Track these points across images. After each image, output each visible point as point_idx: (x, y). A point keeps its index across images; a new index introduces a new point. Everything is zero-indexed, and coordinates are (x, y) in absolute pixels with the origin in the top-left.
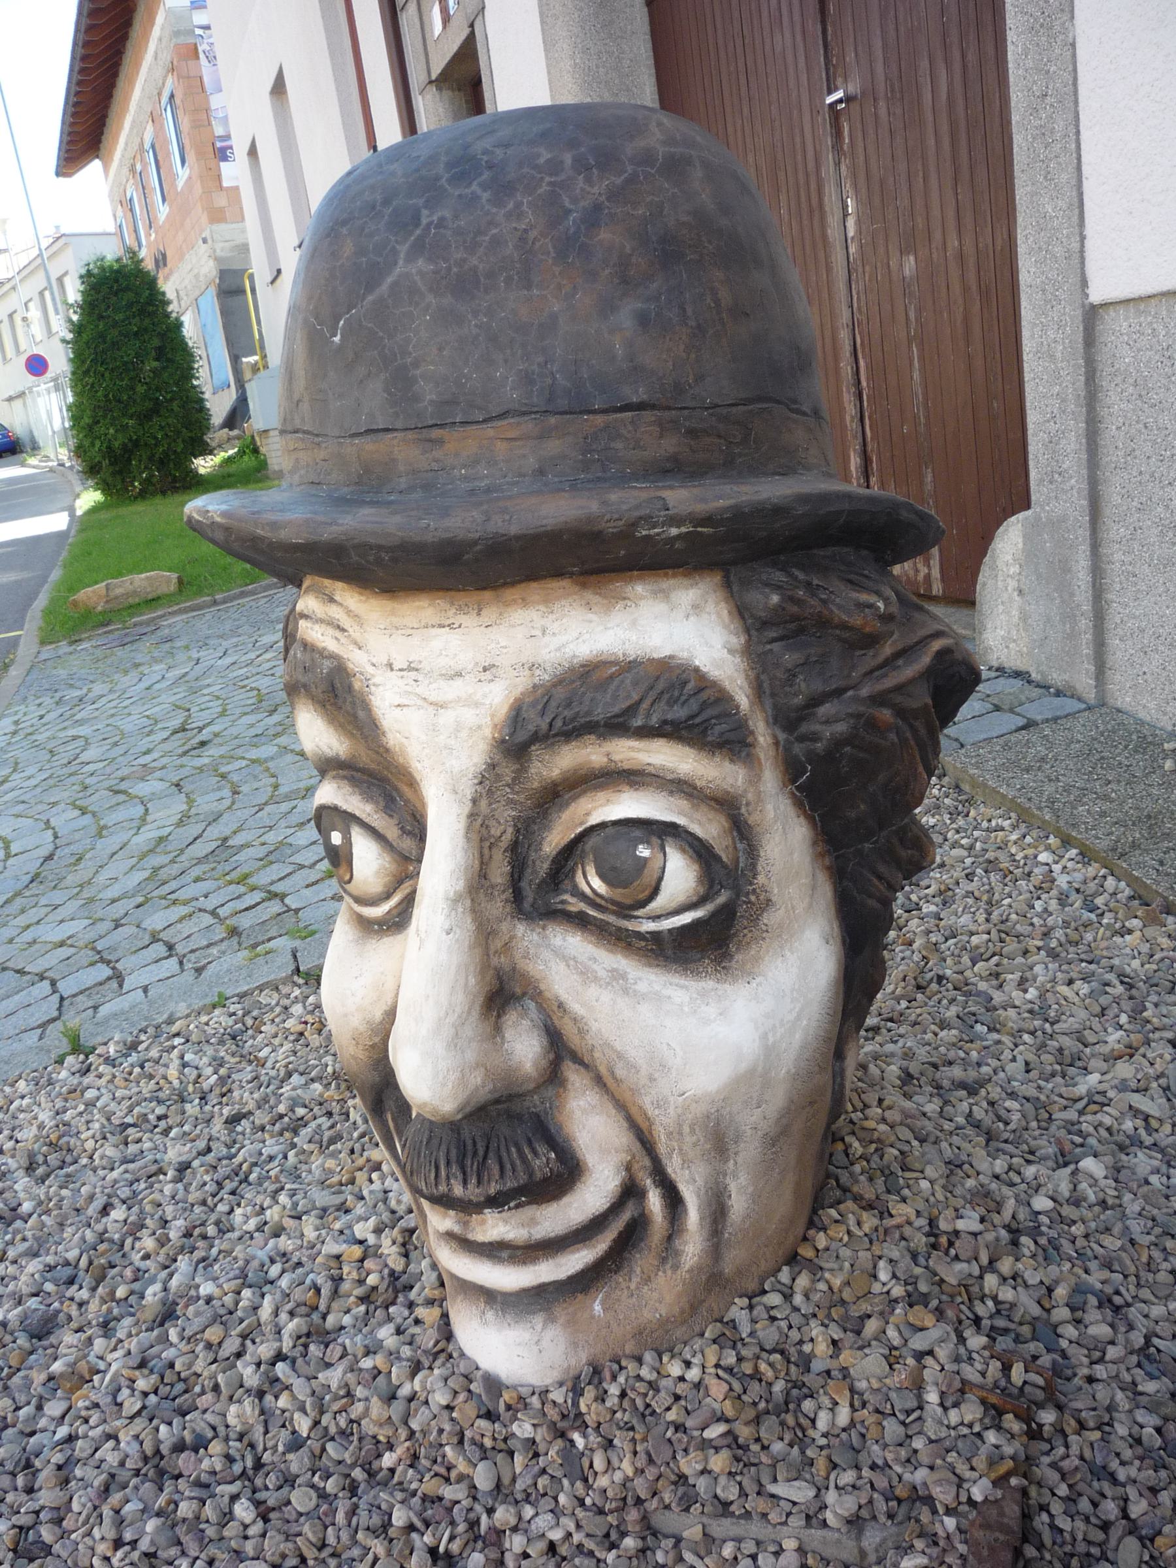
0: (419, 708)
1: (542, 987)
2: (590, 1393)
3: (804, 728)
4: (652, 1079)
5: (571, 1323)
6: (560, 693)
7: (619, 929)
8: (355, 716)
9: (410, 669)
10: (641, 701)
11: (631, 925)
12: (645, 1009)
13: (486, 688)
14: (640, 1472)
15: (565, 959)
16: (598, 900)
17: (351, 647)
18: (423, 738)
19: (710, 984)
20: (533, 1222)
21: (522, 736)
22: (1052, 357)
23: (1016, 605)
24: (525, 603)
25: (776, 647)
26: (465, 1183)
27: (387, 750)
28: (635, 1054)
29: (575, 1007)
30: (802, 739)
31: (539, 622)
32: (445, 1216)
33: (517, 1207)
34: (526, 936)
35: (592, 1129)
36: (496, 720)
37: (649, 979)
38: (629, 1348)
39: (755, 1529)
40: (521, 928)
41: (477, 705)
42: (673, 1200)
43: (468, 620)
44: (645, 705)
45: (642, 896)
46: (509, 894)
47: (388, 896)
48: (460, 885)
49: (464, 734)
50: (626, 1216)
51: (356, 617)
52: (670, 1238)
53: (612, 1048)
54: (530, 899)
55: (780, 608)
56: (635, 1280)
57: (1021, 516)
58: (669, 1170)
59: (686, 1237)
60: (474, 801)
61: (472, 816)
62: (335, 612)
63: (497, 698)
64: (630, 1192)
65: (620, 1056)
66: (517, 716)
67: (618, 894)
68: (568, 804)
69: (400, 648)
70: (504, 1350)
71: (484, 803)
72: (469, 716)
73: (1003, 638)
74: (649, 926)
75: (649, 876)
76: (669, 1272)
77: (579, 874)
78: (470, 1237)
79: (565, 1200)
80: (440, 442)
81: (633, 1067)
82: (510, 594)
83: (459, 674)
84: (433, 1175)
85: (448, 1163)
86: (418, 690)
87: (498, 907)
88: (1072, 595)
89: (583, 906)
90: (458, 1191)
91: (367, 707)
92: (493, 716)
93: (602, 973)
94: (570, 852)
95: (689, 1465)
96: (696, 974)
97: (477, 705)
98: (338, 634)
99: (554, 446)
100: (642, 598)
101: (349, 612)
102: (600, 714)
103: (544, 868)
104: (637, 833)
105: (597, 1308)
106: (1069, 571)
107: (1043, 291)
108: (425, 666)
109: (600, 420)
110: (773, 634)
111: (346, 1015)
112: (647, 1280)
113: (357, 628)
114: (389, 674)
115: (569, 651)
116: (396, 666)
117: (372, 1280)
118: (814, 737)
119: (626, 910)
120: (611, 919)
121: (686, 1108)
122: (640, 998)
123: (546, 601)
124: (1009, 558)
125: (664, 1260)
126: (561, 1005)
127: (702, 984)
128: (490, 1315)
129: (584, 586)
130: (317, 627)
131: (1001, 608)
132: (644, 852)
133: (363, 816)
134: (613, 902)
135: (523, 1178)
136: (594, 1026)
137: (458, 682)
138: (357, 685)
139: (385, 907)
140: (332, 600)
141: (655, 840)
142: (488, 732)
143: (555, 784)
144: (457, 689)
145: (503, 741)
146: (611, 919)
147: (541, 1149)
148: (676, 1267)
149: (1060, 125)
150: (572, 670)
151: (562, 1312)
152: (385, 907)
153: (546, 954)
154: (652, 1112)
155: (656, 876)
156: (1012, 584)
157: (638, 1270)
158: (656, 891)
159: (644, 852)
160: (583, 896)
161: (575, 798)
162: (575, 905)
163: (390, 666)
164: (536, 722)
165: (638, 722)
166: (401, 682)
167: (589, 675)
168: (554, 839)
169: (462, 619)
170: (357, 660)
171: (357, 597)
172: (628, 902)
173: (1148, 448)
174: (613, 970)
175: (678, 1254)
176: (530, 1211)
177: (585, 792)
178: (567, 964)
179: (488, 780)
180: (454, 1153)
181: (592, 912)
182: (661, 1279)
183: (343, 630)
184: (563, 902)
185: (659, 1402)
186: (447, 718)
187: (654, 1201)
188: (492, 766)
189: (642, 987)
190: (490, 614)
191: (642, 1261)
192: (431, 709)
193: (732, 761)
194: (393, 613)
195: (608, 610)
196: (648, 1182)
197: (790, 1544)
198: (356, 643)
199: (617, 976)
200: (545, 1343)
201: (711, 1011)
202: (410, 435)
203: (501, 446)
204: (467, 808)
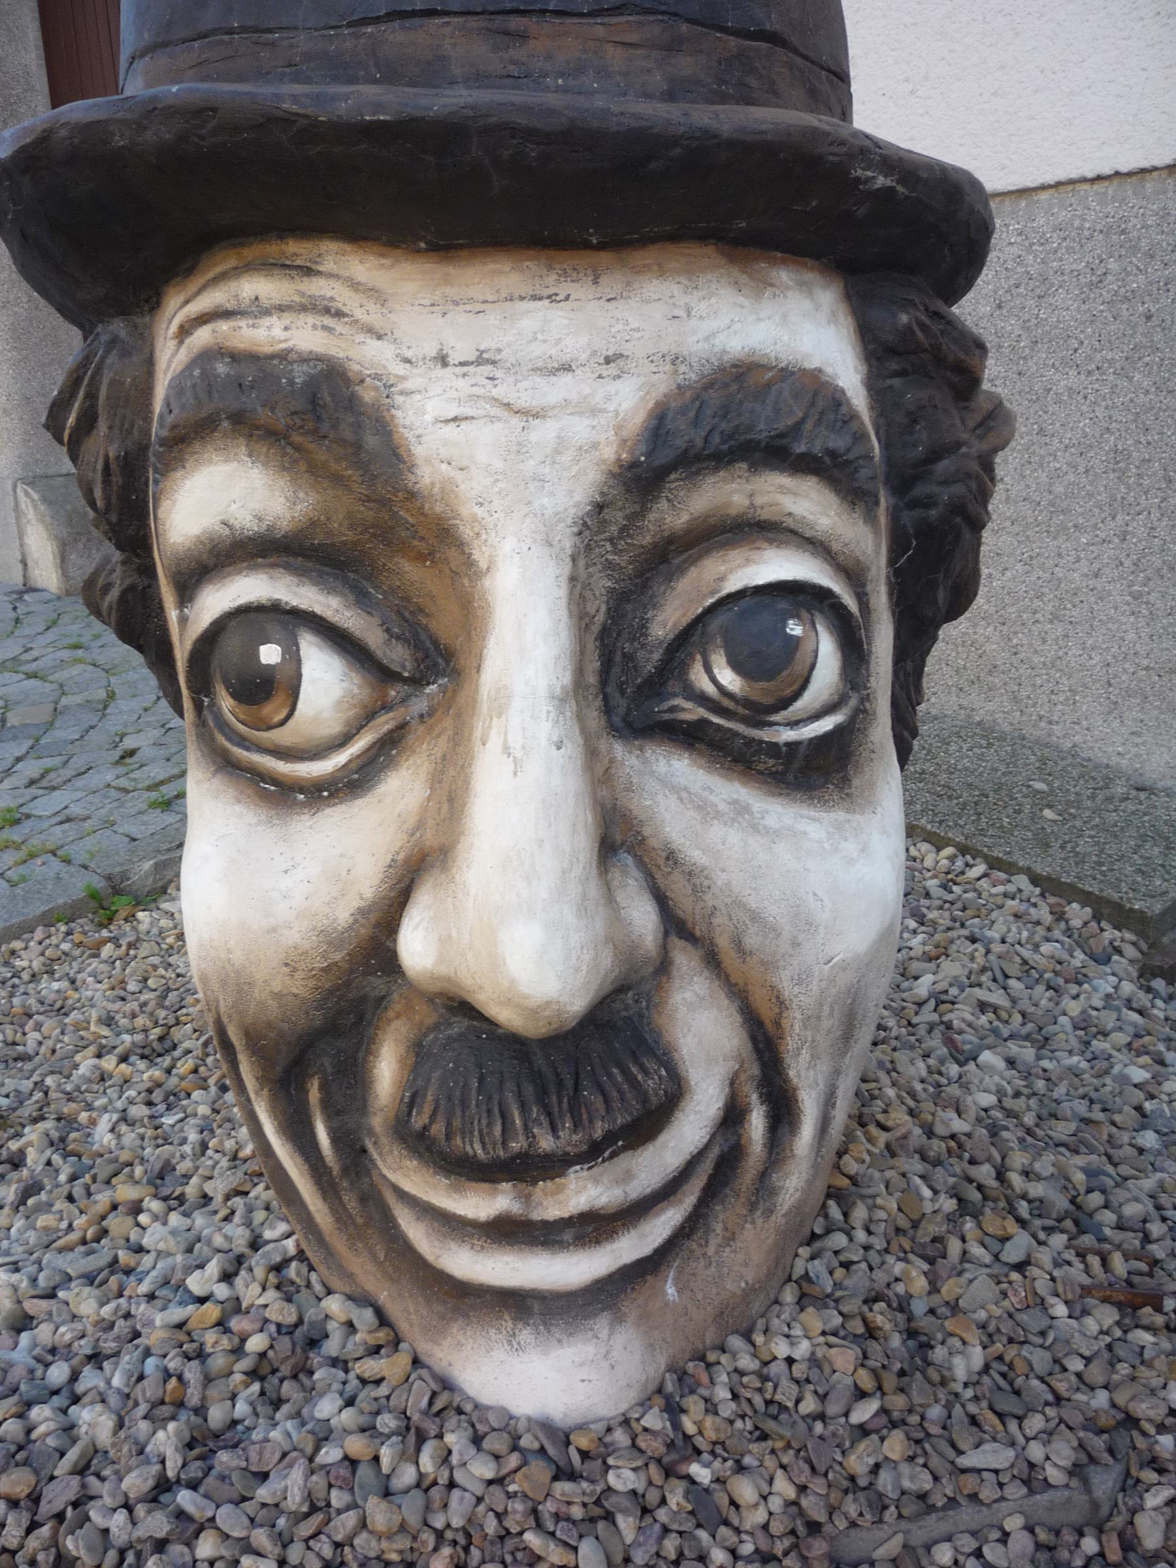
0: (493, 419)
1: (647, 831)
2: (694, 1405)
3: (919, 490)
4: (795, 944)
5: (644, 1318)
6: (715, 398)
7: (749, 742)
8: (358, 446)
9: (481, 361)
10: (802, 421)
11: (766, 735)
12: (782, 848)
13: (612, 387)
14: (802, 1489)
15: (676, 790)
16: (726, 703)
17: (360, 338)
18: (498, 464)
19: (840, 815)
20: (628, 1176)
21: (665, 456)
24: (662, 272)
25: (896, 382)
26: (554, 1129)
27: (412, 495)
28: (774, 911)
29: (695, 855)
30: (913, 504)
31: (682, 299)
32: (494, 1194)
33: (613, 1155)
34: (628, 759)
35: (701, 1033)
36: (625, 433)
37: (779, 813)
38: (710, 1337)
39: (967, 1516)
40: (619, 749)
41: (595, 412)
42: (782, 1112)
43: (580, 290)
44: (808, 426)
45: (788, 692)
46: (599, 702)
47: (344, 740)
48: (567, 679)
49: (566, 458)
50: (715, 1152)
52: (764, 1175)
53: (743, 906)
54: (622, 710)
55: (909, 329)
56: (714, 1242)
58: (792, 1073)
59: (791, 1166)
60: (574, 559)
61: (573, 579)
62: (318, 287)
63: (628, 401)
64: (732, 1116)
65: (755, 917)
66: (659, 426)
67: (760, 691)
68: (682, 570)
69: (461, 333)
70: (540, 1380)
71: (582, 563)
72: (580, 429)
74: (788, 735)
75: (799, 667)
76: (759, 1222)
78: (536, 1215)
79: (662, 1138)
80: (523, 36)
81: (773, 930)
82: (649, 256)
83: (567, 368)
84: (497, 1130)
85: (524, 1108)
86: (495, 392)
87: (594, 718)
89: (702, 712)
90: (546, 1143)
91: (384, 428)
92: (619, 428)
93: (722, 807)
94: (689, 640)
95: (859, 1462)
96: (824, 803)
97: (595, 412)
98: (328, 321)
99: (686, 65)
100: (788, 288)
101: (355, 286)
102: (762, 431)
103: (650, 660)
104: (783, 605)
105: (670, 1290)
109: (733, 42)
110: (894, 366)
111: (274, 930)
112: (730, 1238)
113: (371, 306)
114: (439, 372)
115: (720, 341)
116: (455, 357)
117: (256, 1343)
118: (928, 502)
119: (758, 712)
120: (740, 728)
121: (832, 981)
122: (774, 835)
123: (689, 272)
125: (753, 1207)
126: (672, 857)
127: (833, 815)
128: (525, 1335)
129: (732, 259)
130: (266, 321)
132: (795, 629)
133: (328, 614)
134: (746, 703)
135: (636, 1107)
136: (720, 878)
137: (565, 379)
138: (367, 395)
139: (340, 758)
140: (309, 271)
141: (805, 615)
142: (609, 453)
143: (671, 540)
144: (563, 388)
145: (634, 464)
146: (740, 728)
147: (651, 1065)
150: (722, 369)
151: (631, 1306)
152: (340, 758)
153: (652, 785)
154: (788, 990)
155: (808, 663)
157: (719, 1228)
158: (806, 682)
159: (795, 629)
160: (702, 699)
161: (694, 561)
162: (692, 712)
163: (443, 360)
164: (686, 435)
165: (800, 448)
166: (461, 383)
167: (741, 379)
168: (669, 616)
169: (564, 289)
170: (367, 355)
171: (372, 261)
172: (768, 700)
174: (735, 802)
175: (773, 1192)
176: (626, 1161)
177: (707, 552)
178: (680, 794)
179: (597, 528)
180: (529, 1090)
181: (716, 720)
182: (749, 1233)
183: (339, 314)
184: (673, 709)
185: (786, 1394)
186: (544, 433)
187: (757, 1123)
188: (600, 507)
189: (771, 821)
190: (612, 282)
191: (722, 1216)
192: (516, 422)
193: (865, 522)
194: (447, 280)
195: (758, 295)
196: (754, 1097)
197: (1013, 1523)
198: (370, 330)
199: (741, 810)
200: (616, 1354)
201: (850, 847)
202: (474, 22)
203: (615, 57)
204: (567, 569)
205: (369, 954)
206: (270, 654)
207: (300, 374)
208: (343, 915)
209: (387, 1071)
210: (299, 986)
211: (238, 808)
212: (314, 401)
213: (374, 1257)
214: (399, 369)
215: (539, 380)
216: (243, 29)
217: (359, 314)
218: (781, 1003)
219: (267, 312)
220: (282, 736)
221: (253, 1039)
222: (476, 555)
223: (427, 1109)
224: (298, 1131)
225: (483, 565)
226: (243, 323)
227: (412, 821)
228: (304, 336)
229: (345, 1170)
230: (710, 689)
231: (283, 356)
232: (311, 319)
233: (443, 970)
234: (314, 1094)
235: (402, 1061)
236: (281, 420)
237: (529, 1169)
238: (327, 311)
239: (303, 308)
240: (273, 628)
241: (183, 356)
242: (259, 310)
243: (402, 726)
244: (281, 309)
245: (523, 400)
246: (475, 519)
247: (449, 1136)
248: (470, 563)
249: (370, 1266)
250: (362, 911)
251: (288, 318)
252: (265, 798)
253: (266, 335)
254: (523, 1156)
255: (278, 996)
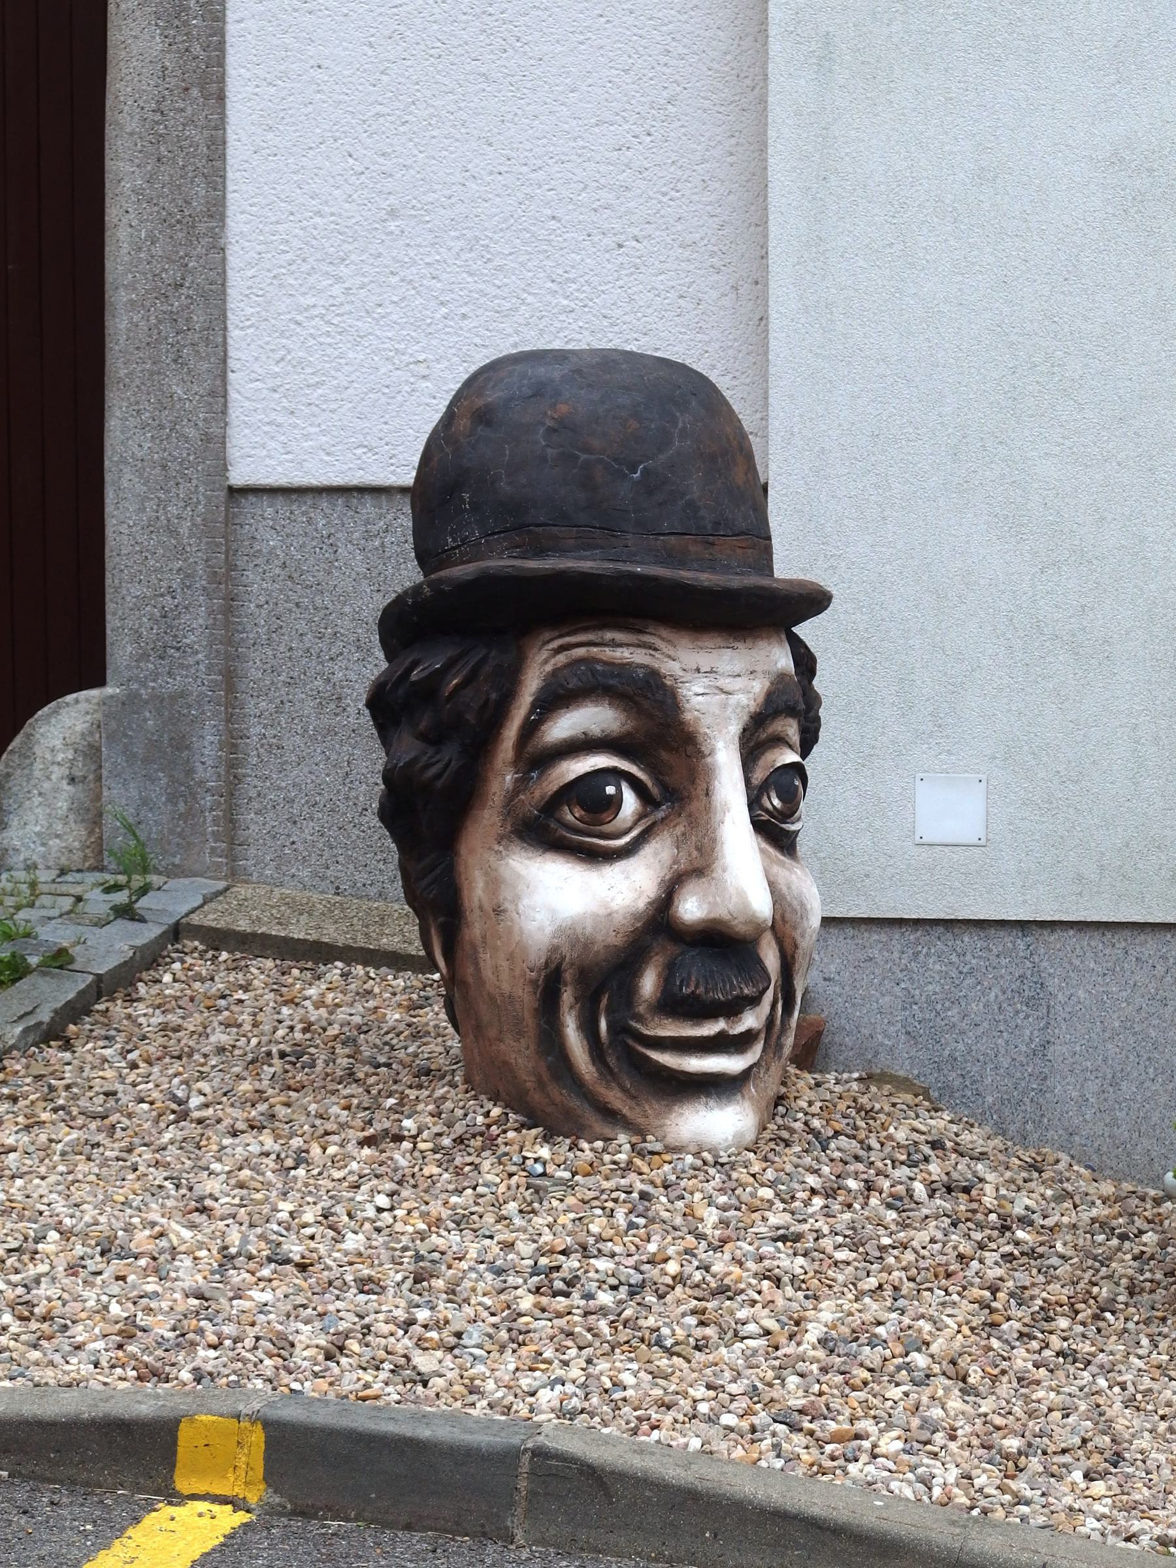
8: (663, 703)
9: (711, 672)
16: (776, 814)
18: (717, 712)
22: (173, 532)
23: (65, 795)
47: (630, 830)
49: (738, 711)
51: (669, 642)
57: (94, 693)
69: (704, 659)
72: (743, 699)
73: (38, 834)
77: (765, 798)
80: (713, 544)
88: (190, 772)
90: (746, 991)
106: (188, 747)
107: (164, 467)
108: (720, 670)
111: (610, 915)
114: (697, 675)
124: (58, 743)
128: (712, 1103)
130: (621, 649)
131: (37, 800)
139: (626, 839)
140: (640, 632)
142: (752, 709)
148: (780, 1057)
149: (199, 318)
152: (626, 839)
156: (57, 773)
160: (767, 811)
161: (763, 754)
163: (698, 670)
168: (759, 776)
169: (736, 644)
170: (669, 667)
173: (302, 626)
186: (733, 700)
190: (749, 643)
205: (659, 921)
206: (610, 790)
207: (641, 673)
208: (641, 904)
209: (649, 984)
210: (618, 941)
211: (570, 865)
212: (648, 682)
213: (624, 1090)
214: (681, 673)
215: (731, 679)
216: (600, 528)
217: (665, 650)
218: (796, 946)
219: (621, 645)
220: (607, 828)
221: (584, 974)
222: (703, 749)
223: (693, 985)
224: (589, 1028)
225: (707, 752)
226: (607, 649)
227: (669, 862)
228: (639, 657)
229: (611, 1043)
230: (770, 807)
231: (630, 664)
232: (644, 651)
233: (712, 916)
234: (604, 1002)
235: (659, 975)
236: (629, 690)
237: (733, 1009)
238: (650, 648)
239: (639, 646)
240: (611, 779)
241: (561, 659)
242: (615, 644)
243: (654, 824)
244: (628, 645)
245: (728, 688)
246: (706, 734)
247: (707, 992)
248: (700, 752)
249: (619, 1094)
250: (649, 903)
251: (632, 649)
252: (582, 860)
253: (623, 654)
254: (737, 997)
255: (607, 947)
